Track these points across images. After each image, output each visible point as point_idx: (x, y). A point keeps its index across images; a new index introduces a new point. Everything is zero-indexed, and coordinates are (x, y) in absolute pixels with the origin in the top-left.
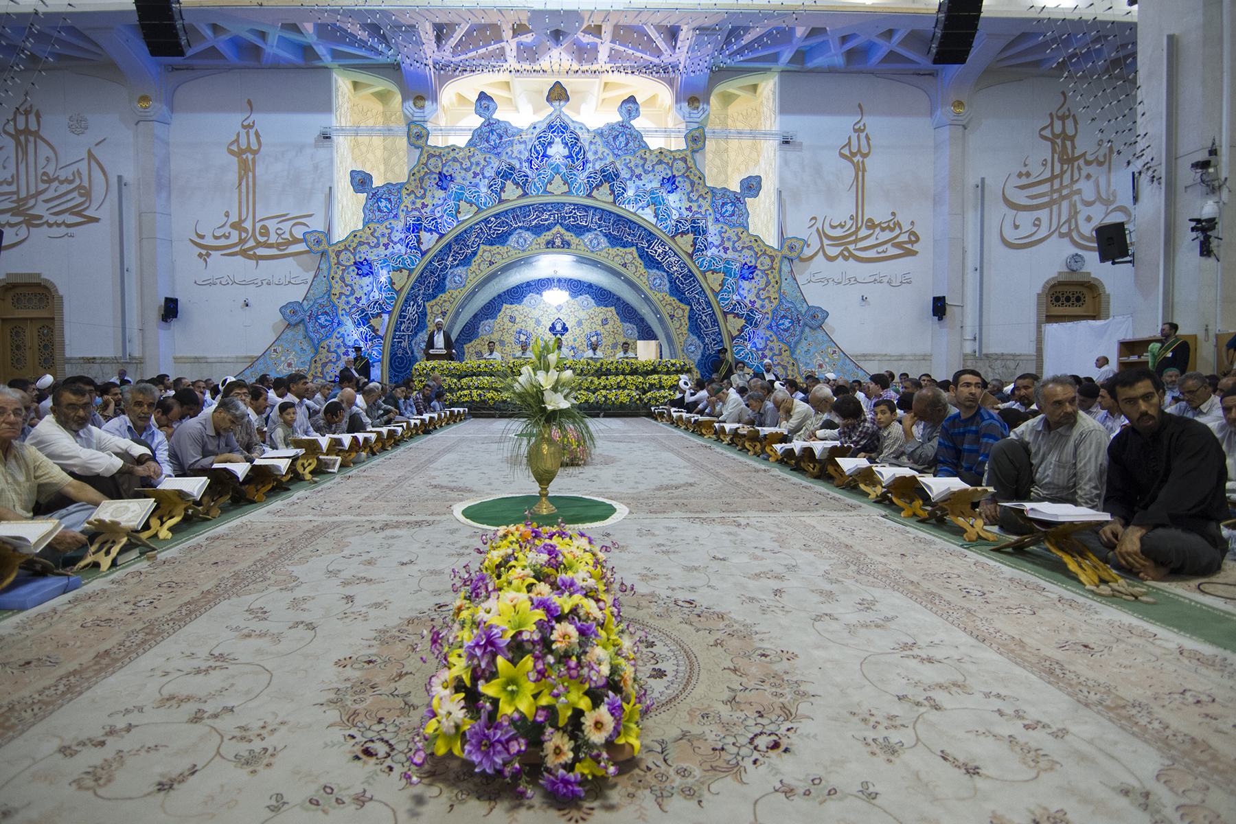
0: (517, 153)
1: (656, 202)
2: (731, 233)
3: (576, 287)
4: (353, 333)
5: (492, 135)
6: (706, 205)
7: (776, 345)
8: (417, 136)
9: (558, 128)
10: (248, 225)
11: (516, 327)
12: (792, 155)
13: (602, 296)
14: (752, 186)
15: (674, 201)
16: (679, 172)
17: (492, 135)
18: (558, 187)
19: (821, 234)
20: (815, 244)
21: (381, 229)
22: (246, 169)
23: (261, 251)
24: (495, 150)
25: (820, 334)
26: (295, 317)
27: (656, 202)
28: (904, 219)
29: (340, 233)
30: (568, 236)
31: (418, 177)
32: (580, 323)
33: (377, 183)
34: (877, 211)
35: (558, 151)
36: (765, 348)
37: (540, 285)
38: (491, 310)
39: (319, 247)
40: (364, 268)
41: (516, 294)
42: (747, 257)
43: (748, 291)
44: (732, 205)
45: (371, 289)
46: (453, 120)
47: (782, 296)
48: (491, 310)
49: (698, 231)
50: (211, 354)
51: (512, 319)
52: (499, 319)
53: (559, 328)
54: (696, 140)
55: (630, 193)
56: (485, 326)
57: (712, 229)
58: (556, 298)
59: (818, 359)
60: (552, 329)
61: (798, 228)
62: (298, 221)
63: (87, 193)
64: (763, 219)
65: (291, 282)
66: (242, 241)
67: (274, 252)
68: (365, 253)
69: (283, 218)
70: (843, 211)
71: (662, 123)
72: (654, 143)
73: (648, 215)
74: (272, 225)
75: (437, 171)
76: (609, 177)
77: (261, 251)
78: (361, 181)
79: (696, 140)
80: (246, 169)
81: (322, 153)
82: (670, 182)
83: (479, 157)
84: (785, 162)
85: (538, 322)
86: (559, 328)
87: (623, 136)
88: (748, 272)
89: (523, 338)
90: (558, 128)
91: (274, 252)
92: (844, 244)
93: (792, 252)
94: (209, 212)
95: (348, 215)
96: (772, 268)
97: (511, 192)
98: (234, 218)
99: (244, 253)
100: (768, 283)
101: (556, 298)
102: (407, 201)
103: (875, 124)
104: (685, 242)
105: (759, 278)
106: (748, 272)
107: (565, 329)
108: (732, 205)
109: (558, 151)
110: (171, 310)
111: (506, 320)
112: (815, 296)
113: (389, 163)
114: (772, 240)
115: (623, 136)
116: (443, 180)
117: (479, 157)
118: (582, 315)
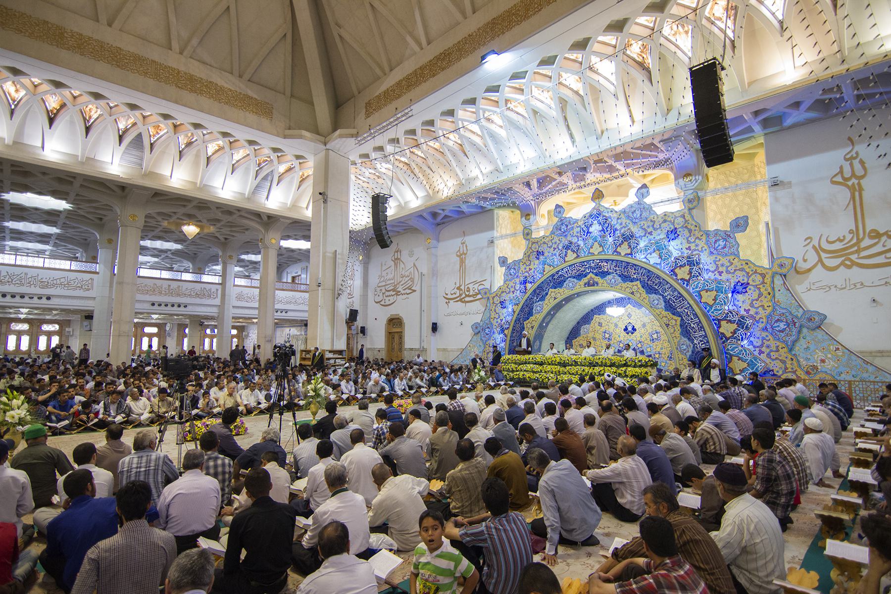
1: (659, 248)
2: (724, 260)
5: (563, 226)
6: (701, 244)
7: (773, 343)
8: (527, 234)
10: (462, 287)
11: (603, 329)
12: (781, 193)
14: (740, 224)
15: (675, 248)
17: (563, 226)
18: (596, 249)
19: (818, 250)
20: (813, 258)
21: (511, 284)
22: (462, 262)
23: (467, 299)
24: (564, 234)
25: (819, 334)
27: (659, 248)
29: (495, 288)
30: (597, 279)
32: (644, 325)
33: (510, 261)
35: (595, 228)
36: (762, 345)
38: (586, 319)
39: (485, 295)
42: (741, 277)
43: (743, 302)
44: (725, 241)
47: (775, 305)
48: (586, 319)
49: (692, 263)
50: (449, 348)
51: (600, 324)
52: (592, 324)
53: (630, 329)
55: (642, 244)
56: (584, 329)
57: (706, 259)
59: (820, 355)
60: (626, 329)
61: (794, 247)
62: (480, 283)
63: (412, 280)
64: (754, 249)
65: (475, 312)
66: (461, 295)
67: (472, 299)
68: (505, 297)
69: (475, 282)
72: (659, 210)
73: (654, 259)
74: (471, 286)
77: (467, 299)
80: (462, 262)
81: (490, 249)
82: (673, 234)
83: (556, 239)
84: (776, 199)
85: (616, 326)
86: (630, 329)
88: (740, 288)
89: (607, 336)
90: (596, 215)
91: (472, 299)
93: (785, 270)
94: (448, 284)
96: (763, 282)
97: (571, 256)
98: (458, 285)
99: (461, 300)
100: (760, 295)
101: (613, 311)
102: (522, 268)
104: (683, 273)
105: (752, 293)
106: (740, 288)
107: (634, 329)
108: (725, 241)
109: (595, 228)
110: (435, 328)
111: (596, 325)
112: (813, 302)
114: (765, 263)
117: (556, 239)
118: (646, 320)
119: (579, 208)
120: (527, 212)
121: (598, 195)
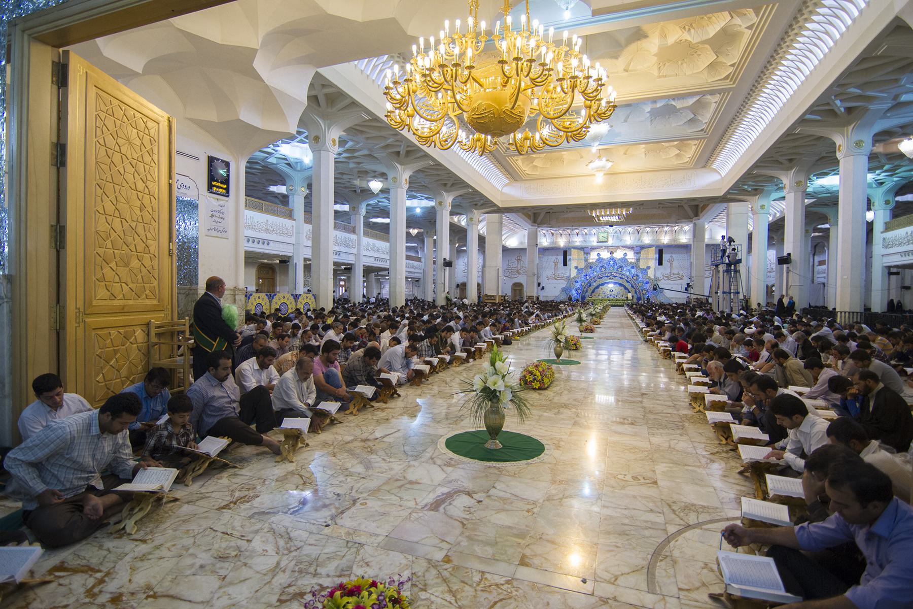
0: (604, 263)
1: (629, 271)
3: (615, 283)
4: (574, 292)
5: (600, 260)
8: (586, 260)
9: (612, 259)
13: (621, 285)
14: (649, 268)
15: (633, 271)
16: (635, 266)
17: (600, 260)
26: (563, 290)
27: (629, 271)
28: (681, 273)
31: (586, 267)
34: (675, 271)
35: (612, 263)
37: (608, 283)
38: (598, 287)
40: (576, 282)
41: (603, 284)
45: (578, 285)
46: (593, 256)
48: (598, 287)
54: (638, 260)
57: (640, 275)
58: (611, 286)
61: (659, 275)
64: (651, 273)
65: (563, 284)
70: (668, 271)
71: (631, 256)
75: (590, 266)
76: (621, 267)
78: (576, 268)
79: (638, 260)
82: (633, 267)
87: (624, 260)
88: (647, 283)
92: (668, 278)
95: (574, 273)
101: (611, 286)
103: (674, 255)
106: (647, 283)
109: (612, 263)
113: (582, 265)
115: (624, 260)
116: (591, 267)
119: (605, 255)
120: (587, 253)
121: (612, 253)
